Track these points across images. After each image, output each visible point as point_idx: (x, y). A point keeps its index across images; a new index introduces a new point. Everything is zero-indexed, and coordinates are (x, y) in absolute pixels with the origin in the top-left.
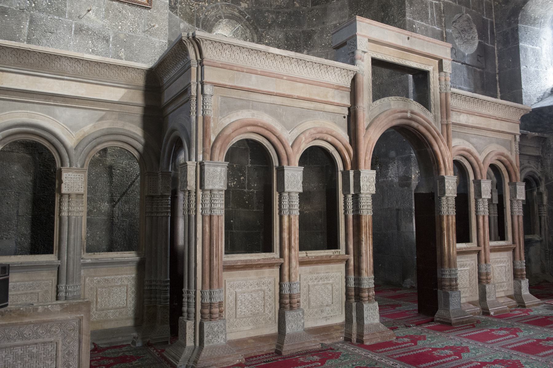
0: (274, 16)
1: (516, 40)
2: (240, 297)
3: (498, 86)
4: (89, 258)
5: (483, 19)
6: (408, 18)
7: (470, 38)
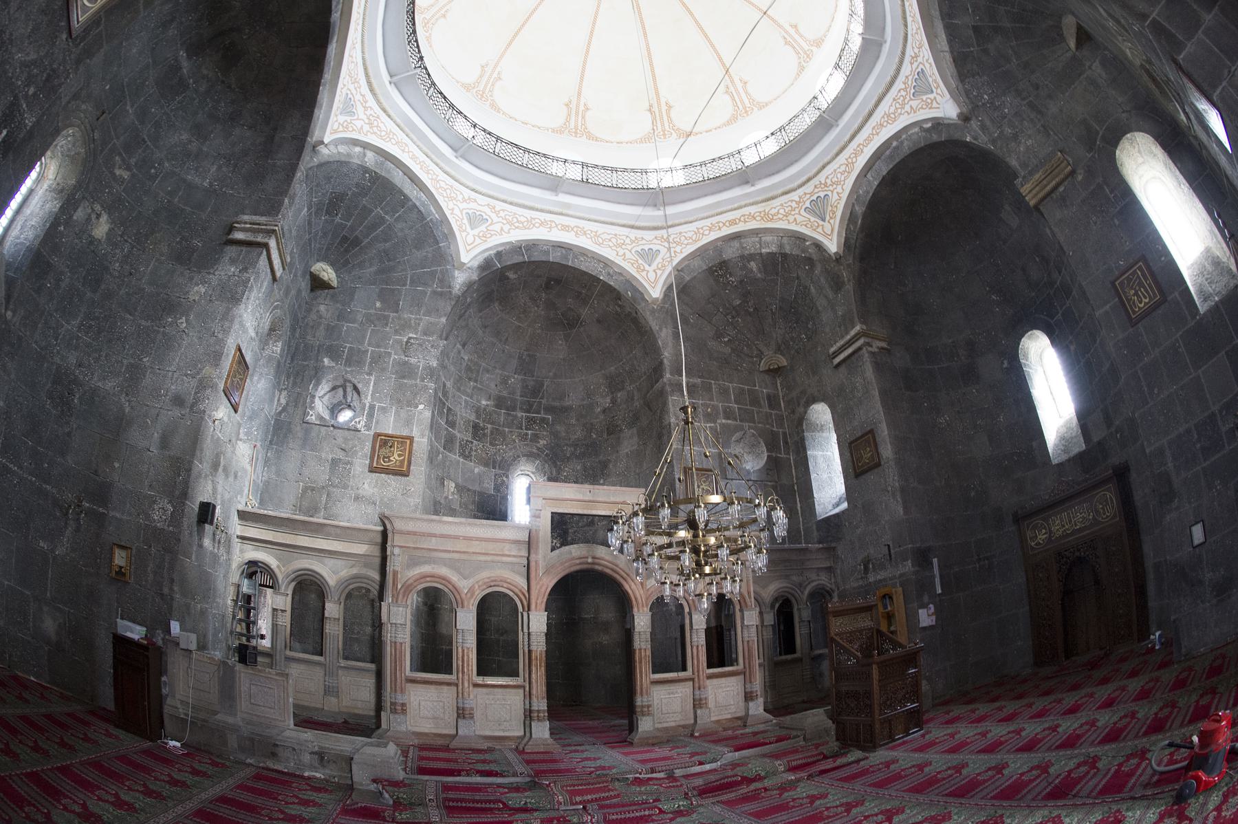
0: (572, 449)
1: (805, 450)
5: (772, 431)
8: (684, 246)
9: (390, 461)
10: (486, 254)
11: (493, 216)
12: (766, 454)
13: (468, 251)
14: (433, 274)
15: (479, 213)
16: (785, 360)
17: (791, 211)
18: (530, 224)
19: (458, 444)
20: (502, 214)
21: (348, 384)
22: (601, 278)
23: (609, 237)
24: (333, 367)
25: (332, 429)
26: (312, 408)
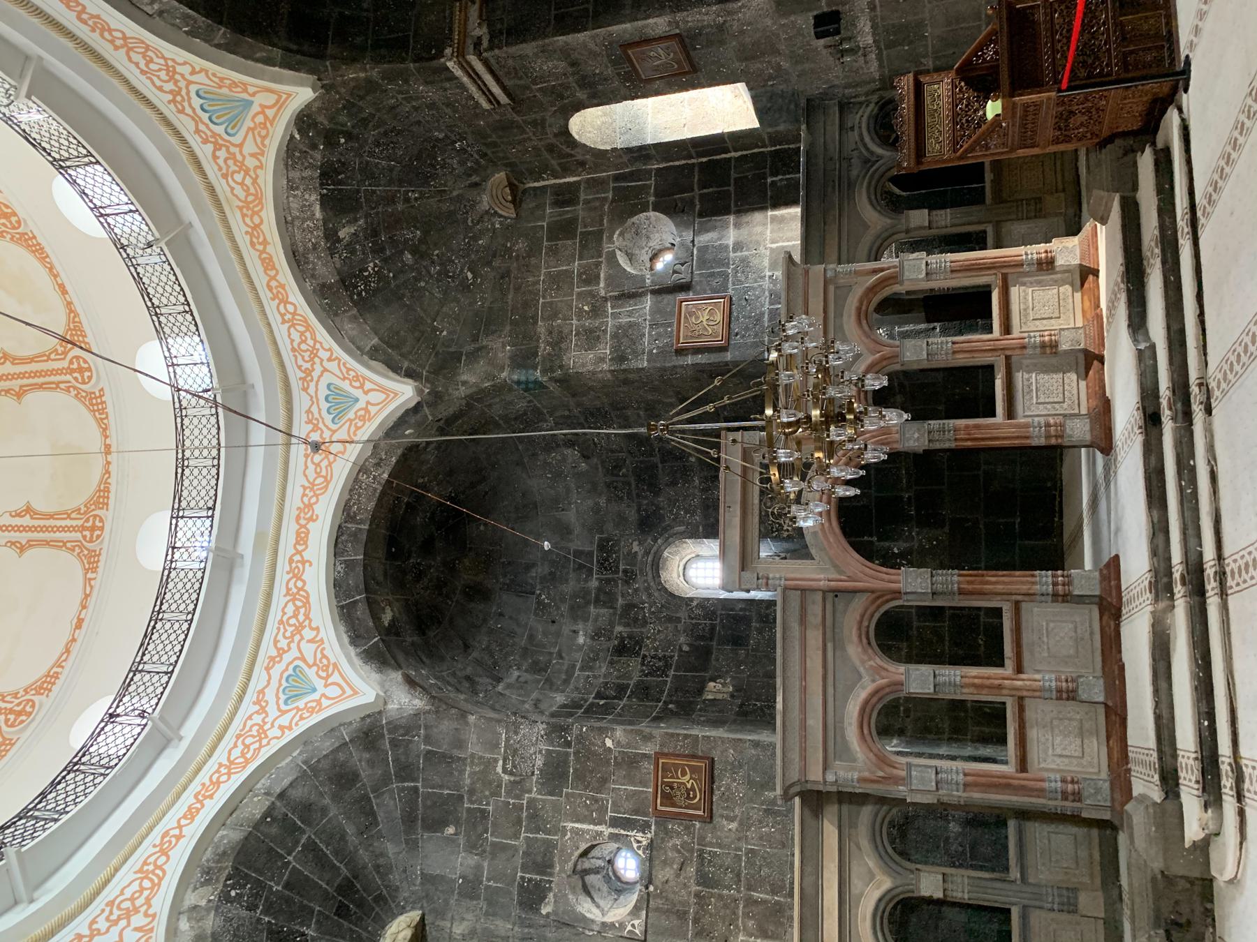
2: (1058, 751)
3: (718, 157)
4: (1015, 873)
5: (613, 201)
6: (645, 364)
7: (647, 222)
8: (318, 346)
9: (693, 789)
10: (358, 662)
11: (287, 658)
12: (652, 214)
13: (355, 693)
14: (395, 744)
15: (283, 682)
16: (497, 175)
17: (236, 161)
18: (299, 596)
19: (649, 678)
20: (283, 643)
21: (579, 867)
22: (386, 476)
23: (311, 467)
24: (555, 896)
25: (651, 888)
26: (622, 925)
